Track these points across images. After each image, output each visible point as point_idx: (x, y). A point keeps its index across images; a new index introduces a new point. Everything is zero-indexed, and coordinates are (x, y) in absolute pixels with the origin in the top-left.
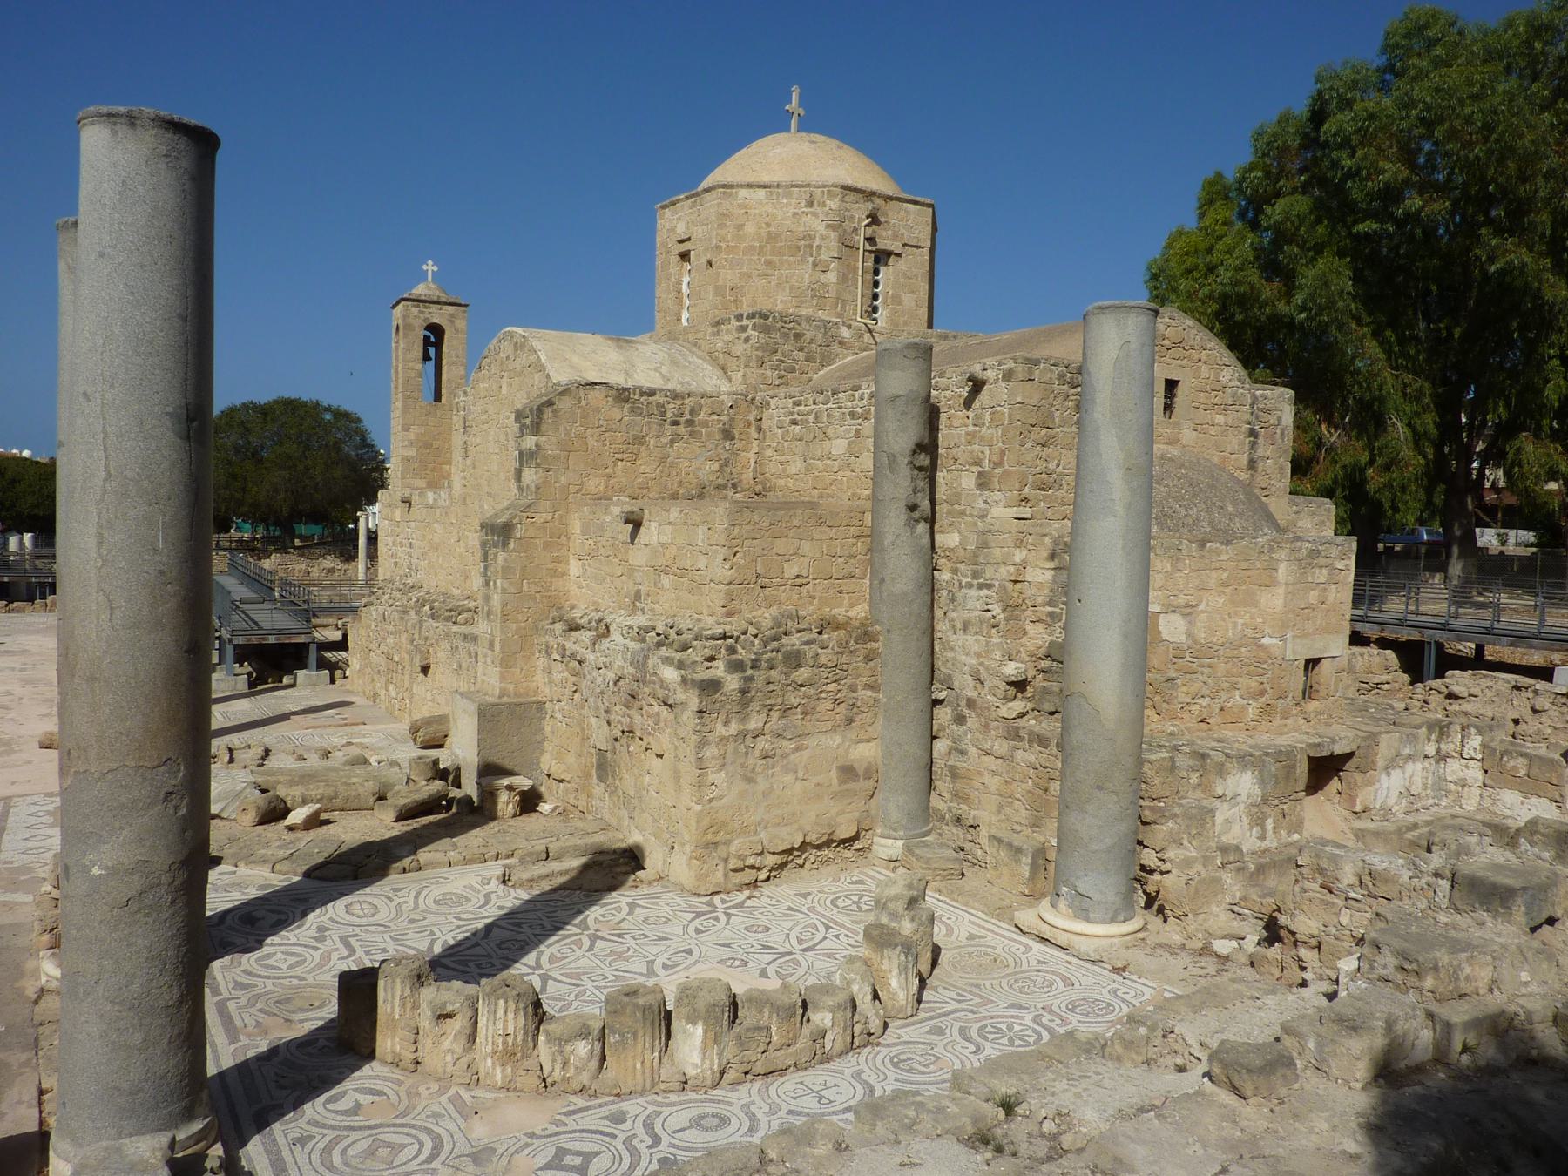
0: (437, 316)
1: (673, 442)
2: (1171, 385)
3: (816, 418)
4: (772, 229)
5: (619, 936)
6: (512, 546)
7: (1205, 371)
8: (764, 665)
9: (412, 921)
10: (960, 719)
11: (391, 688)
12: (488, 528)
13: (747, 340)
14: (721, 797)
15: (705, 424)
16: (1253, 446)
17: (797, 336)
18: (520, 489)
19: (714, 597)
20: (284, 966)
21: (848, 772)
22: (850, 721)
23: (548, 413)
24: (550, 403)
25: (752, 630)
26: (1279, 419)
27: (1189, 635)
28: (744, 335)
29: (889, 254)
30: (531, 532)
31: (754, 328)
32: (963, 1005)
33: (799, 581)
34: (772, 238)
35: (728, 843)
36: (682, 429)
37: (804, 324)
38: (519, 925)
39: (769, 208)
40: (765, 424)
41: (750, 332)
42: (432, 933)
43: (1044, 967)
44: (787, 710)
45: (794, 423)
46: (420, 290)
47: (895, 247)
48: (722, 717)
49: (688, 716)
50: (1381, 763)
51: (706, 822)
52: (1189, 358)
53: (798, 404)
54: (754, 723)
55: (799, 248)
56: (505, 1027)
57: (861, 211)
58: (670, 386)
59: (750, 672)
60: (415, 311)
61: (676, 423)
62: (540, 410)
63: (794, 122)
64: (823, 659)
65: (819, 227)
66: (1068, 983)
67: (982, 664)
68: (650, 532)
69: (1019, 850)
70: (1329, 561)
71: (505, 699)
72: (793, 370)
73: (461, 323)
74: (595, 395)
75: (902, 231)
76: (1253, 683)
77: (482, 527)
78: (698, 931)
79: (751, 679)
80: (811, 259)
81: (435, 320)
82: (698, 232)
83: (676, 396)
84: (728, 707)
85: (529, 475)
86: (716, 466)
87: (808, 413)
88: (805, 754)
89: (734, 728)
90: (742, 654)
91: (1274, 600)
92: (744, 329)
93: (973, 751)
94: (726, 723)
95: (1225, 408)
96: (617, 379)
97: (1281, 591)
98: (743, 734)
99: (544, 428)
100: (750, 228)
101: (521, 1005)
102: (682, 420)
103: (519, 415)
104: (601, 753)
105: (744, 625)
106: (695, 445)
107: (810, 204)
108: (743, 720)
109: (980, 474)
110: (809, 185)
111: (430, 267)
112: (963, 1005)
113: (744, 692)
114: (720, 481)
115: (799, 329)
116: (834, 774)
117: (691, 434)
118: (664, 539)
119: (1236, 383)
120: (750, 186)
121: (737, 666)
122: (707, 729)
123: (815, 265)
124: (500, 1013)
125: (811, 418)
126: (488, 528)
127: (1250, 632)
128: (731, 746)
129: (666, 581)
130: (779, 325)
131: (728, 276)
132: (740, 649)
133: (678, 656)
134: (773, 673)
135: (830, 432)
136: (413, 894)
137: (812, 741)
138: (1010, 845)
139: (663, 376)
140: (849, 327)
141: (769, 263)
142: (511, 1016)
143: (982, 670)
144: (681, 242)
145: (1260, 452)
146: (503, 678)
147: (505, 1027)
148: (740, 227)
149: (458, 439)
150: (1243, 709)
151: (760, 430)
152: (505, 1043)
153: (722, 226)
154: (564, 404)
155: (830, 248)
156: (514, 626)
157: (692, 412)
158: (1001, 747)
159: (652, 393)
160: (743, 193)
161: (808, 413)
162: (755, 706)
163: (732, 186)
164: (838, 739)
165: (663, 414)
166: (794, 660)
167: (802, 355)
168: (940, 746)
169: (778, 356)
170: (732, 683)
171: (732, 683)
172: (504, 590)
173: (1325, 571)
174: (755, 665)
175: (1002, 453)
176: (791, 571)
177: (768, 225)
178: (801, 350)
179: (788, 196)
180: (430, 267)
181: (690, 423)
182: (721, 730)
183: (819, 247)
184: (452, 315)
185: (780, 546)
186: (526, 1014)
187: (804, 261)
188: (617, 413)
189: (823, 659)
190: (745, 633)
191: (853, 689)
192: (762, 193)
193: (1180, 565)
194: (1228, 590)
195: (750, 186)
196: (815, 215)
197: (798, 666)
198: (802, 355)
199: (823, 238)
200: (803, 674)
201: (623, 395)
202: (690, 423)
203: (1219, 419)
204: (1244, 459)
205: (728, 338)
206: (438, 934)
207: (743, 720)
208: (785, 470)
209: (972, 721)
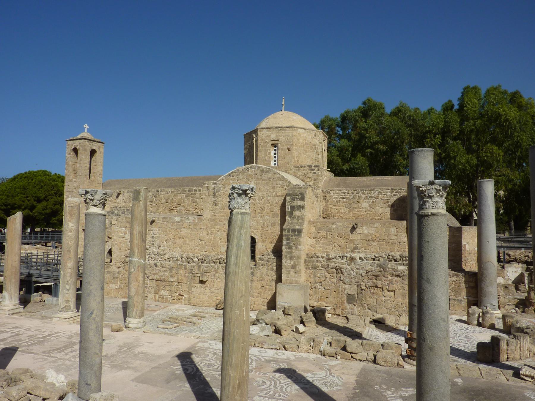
0: (95, 146)
28: (313, 172)
34: (306, 144)
39: (305, 135)
40: (328, 198)
41: (316, 171)
46: (85, 134)
60: (88, 143)
63: (283, 108)
69: (461, 300)
73: (102, 150)
81: (94, 148)
92: (313, 170)
100: (301, 140)
107: (315, 136)
111: (86, 126)
120: (301, 128)
129: (374, 244)
138: (458, 300)
141: (305, 151)
148: (298, 139)
160: (299, 130)
163: (296, 128)
179: (310, 132)
180: (86, 126)
184: (99, 146)
192: (304, 130)
195: (301, 128)
199: (318, 145)
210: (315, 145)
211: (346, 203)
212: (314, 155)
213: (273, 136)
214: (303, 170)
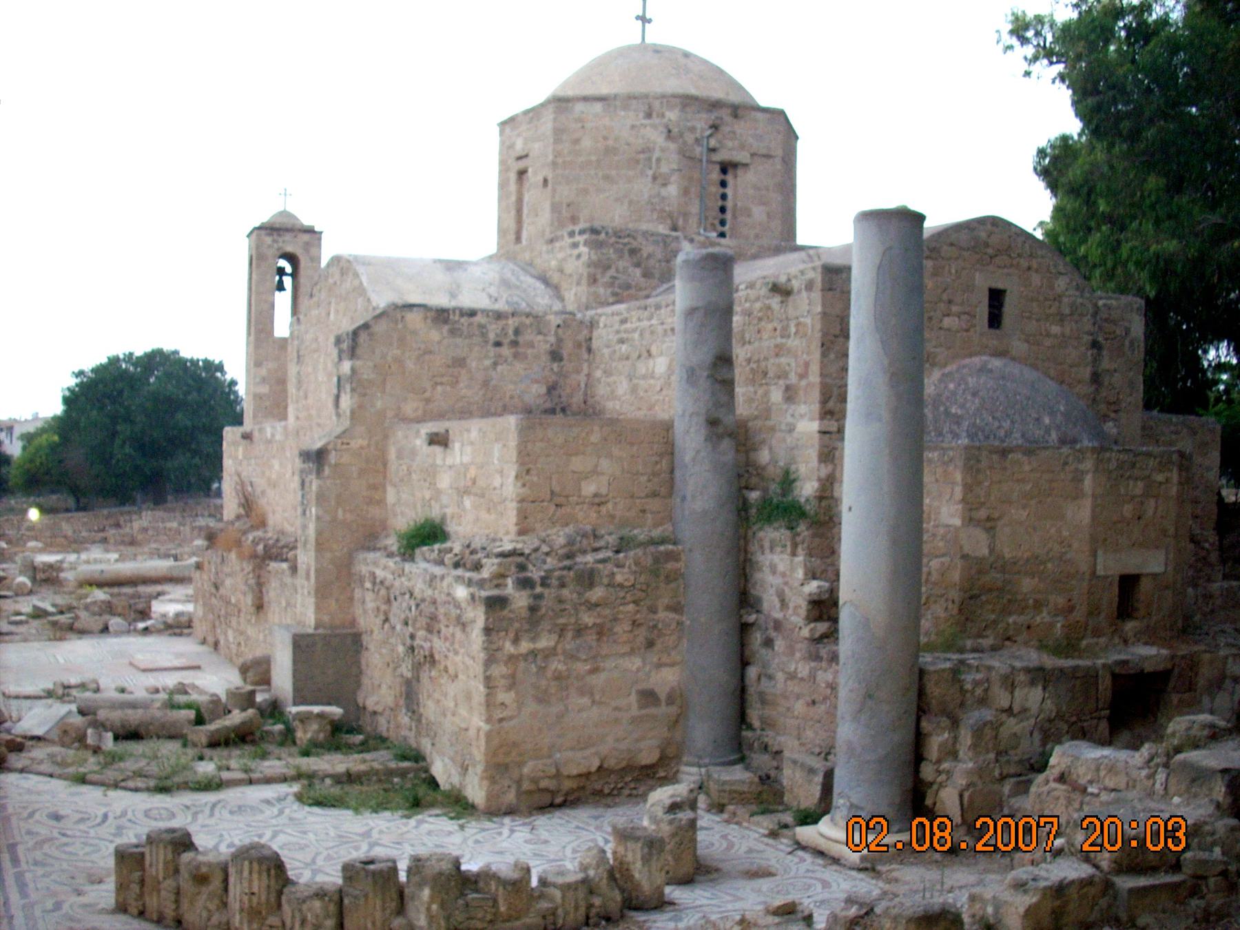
1: (495, 364)
2: (996, 297)
3: (641, 335)
4: (610, 143)
5: (398, 843)
6: (327, 471)
7: (1036, 279)
8: (554, 582)
9: (203, 826)
10: (768, 643)
11: (230, 632)
12: (306, 456)
13: (579, 256)
14: (511, 718)
15: (531, 345)
16: (1096, 360)
17: (633, 252)
18: (338, 415)
19: (510, 519)
20: (81, 853)
21: (649, 697)
22: (650, 644)
23: (363, 337)
24: (366, 326)
25: (545, 549)
26: (1127, 331)
27: (992, 550)
28: (576, 252)
29: (735, 165)
30: (346, 459)
31: (585, 243)
32: (713, 902)
33: (597, 500)
34: (609, 151)
35: (520, 765)
36: (506, 351)
37: (640, 239)
38: (305, 833)
39: (607, 121)
42: (221, 836)
43: (810, 874)
44: (580, 631)
45: (622, 341)
47: (741, 157)
48: (512, 635)
49: (476, 636)
50: (1201, 682)
51: (496, 742)
52: (1018, 266)
53: (624, 321)
54: (544, 642)
55: (638, 162)
56: (250, 887)
57: (701, 122)
58: (497, 307)
59: (538, 590)
60: (268, 240)
61: (498, 344)
62: (355, 333)
64: (619, 578)
65: (658, 138)
66: (826, 884)
67: (786, 583)
68: (459, 454)
70: (1147, 473)
71: (321, 631)
72: (628, 287)
74: (413, 318)
75: (751, 140)
76: (1061, 601)
77: (301, 455)
78: (477, 842)
79: (539, 597)
80: (650, 173)
82: (536, 147)
83: (499, 316)
84: (517, 625)
85: (346, 401)
86: (543, 390)
87: (634, 330)
88: (603, 676)
89: (525, 646)
90: (535, 574)
91: (1081, 513)
92: (575, 245)
93: (780, 676)
94: (516, 641)
95: (1061, 319)
96: (442, 301)
97: (1087, 503)
98: (533, 653)
99: (359, 351)
100: (587, 143)
101: (264, 867)
102: (506, 341)
103: (338, 341)
104: (408, 683)
105: (536, 543)
106: (519, 366)
107: (649, 116)
108: (533, 640)
109: (788, 388)
110: (646, 96)
112: (713, 902)
113: (533, 609)
114: (548, 405)
115: (635, 244)
116: (633, 698)
117: (516, 356)
118: (466, 459)
119: (1071, 292)
121: (525, 583)
122: (494, 647)
123: (655, 178)
124: (246, 873)
125: (636, 336)
126: (306, 456)
127: (1056, 547)
128: (522, 665)
129: (468, 502)
130: (613, 239)
131: (566, 193)
132: (530, 567)
133: (468, 575)
134: (565, 592)
135: (654, 350)
136: (210, 805)
137: (610, 664)
139: (490, 297)
140: (692, 241)
142: (255, 876)
143: (787, 590)
144: (520, 158)
145: (1106, 364)
146: (318, 608)
147: (250, 887)
148: (577, 141)
149: (293, 369)
150: (1051, 625)
151: (589, 350)
152: (250, 901)
153: (557, 141)
154: (380, 328)
155: (670, 162)
156: (328, 555)
157: (517, 332)
158: (804, 670)
159: (472, 313)
160: (579, 107)
161: (634, 330)
162: (546, 625)
164: (637, 662)
165: (484, 335)
166: (588, 579)
167: (638, 272)
168: (752, 672)
169: (612, 272)
170: (521, 600)
171: (521, 600)
172: (318, 518)
173: (1140, 484)
174: (544, 582)
175: (807, 365)
176: (589, 489)
177: (605, 138)
178: (638, 265)
179: (626, 107)
181: (515, 344)
182: (509, 648)
183: (658, 160)
185: (577, 463)
186: (269, 875)
187: (642, 173)
188: (435, 335)
189: (619, 578)
190: (536, 550)
191: (653, 610)
192: (598, 107)
193: (981, 477)
194: (1033, 502)
195: (586, 99)
196: (654, 127)
197: (591, 585)
198: (638, 272)
199: (663, 150)
200: (597, 593)
201: (441, 316)
202: (515, 344)
203: (1055, 329)
204: (1086, 373)
205: (560, 256)
206: (226, 836)
207: (533, 640)
208: (613, 392)
209: (779, 644)
210: (647, 150)
211: (627, 358)
212: (643, 188)
213: (519, 146)
214: (561, 248)
